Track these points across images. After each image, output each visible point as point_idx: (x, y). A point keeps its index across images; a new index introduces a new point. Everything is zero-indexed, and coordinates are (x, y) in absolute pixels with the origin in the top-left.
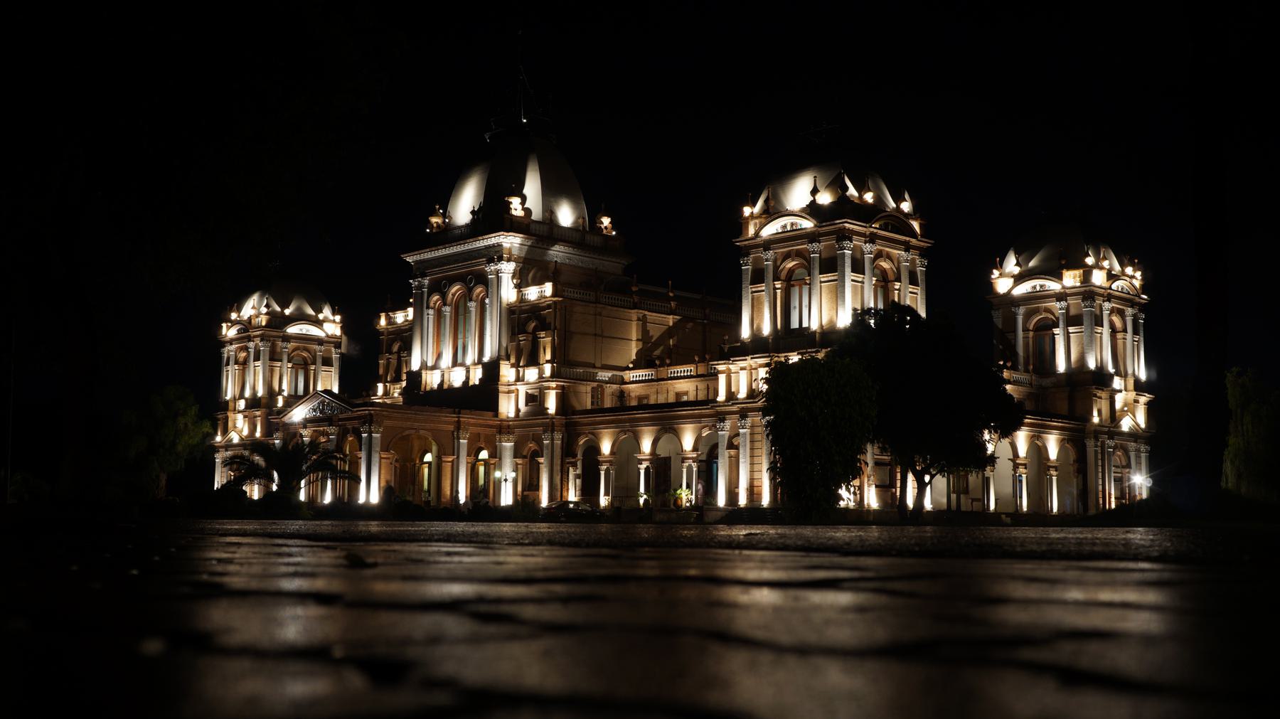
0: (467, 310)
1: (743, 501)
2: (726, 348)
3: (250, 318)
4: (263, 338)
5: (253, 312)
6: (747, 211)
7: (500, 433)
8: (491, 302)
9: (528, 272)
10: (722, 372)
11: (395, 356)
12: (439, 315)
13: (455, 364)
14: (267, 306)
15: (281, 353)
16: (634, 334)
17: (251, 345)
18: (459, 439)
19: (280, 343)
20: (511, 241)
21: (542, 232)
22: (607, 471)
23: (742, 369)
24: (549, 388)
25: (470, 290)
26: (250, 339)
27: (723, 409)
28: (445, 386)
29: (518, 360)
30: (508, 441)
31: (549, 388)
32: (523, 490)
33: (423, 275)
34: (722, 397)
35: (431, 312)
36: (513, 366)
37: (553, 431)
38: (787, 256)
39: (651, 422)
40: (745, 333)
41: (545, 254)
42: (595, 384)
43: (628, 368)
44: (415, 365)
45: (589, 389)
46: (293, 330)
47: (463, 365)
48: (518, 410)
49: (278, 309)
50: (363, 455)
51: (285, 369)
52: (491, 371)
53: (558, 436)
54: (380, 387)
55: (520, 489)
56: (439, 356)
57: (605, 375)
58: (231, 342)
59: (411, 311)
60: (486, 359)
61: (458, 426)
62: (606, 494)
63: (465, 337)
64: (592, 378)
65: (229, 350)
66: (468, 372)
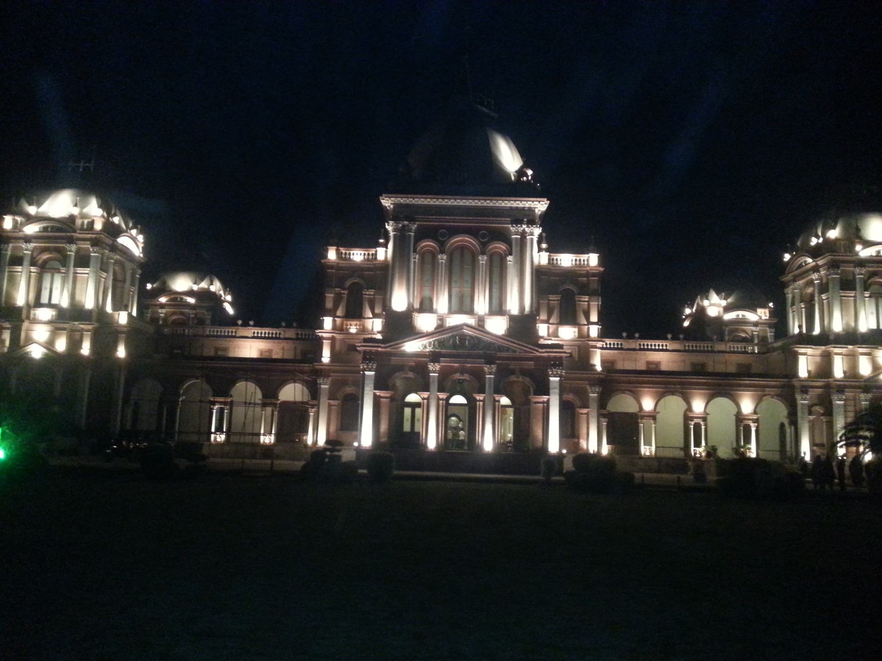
24: (596, 347)
31: (596, 347)
66: (481, 320)
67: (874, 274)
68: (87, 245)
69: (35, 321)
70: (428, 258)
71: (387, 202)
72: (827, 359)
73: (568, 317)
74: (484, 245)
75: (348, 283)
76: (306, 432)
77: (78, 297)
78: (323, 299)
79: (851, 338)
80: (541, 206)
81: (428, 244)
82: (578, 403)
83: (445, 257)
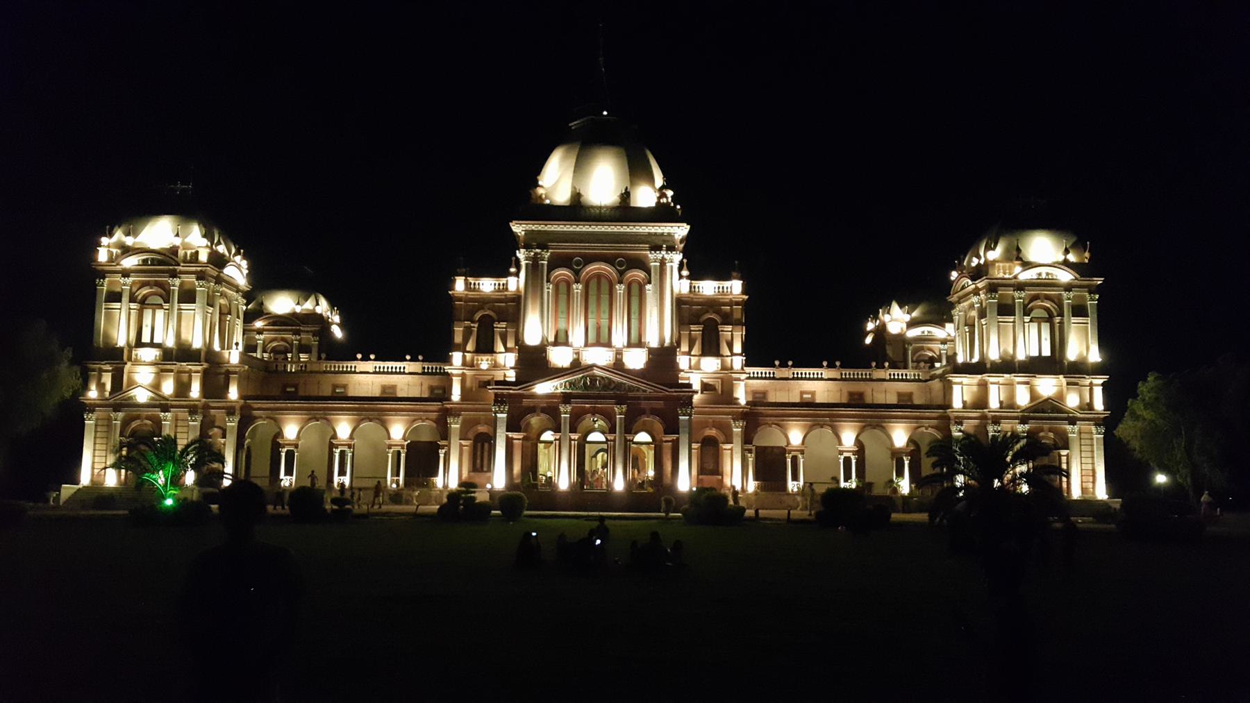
24: (739, 379)
29: (691, 348)
31: (739, 379)
54: (457, 357)
66: (619, 353)
67: (1035, 298)
68: (192, 279)
69: (137, 362)
70: (563, 287)
71: (518, 228)
72: (984, 386)
73: (711, 347)
74: (621, 273)
75: (477, 316)
76: (435, 474)
77: (184, 336)
78: (451, 334)
79: (1007, 366)
80: (680, 231)
82: (721, 438)
83: (580, 286)
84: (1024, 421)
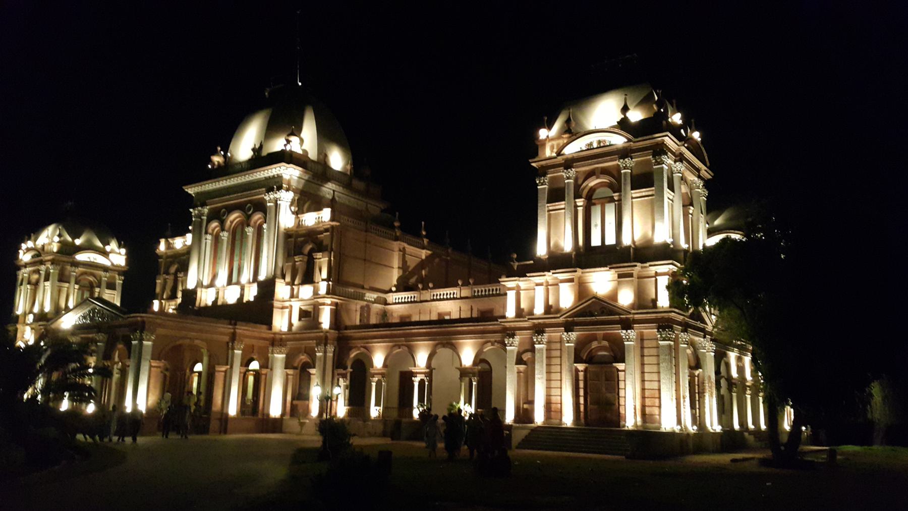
0: (244, 235)
1: (539, 418)
2: (516, 265)
3: (43, 246)
4: (53, 262)
5: (47, 241)
6: (543, 133)
7: (273, 345)
8: (269, 228)
9: (307, 200)
10: (510, 289)
11: (170, 278)
12: (217, 240)
13: (230, 282)
14: (60, 236)
15: (70, 276)
16: (396, 262)
17: (43, 268)
18: (233, 349)
19: (69, 267)
20: (291, 173)
21: (317, 170)
22: (379, 384)
23: (537, 285)
24: (324, 304)
25: (249, 217)
26: (42, 263)
27: (512, 324)
28: (219, 303)
29: (293, 279)
30: (280, 353)
31: (324, 304)
32: (293, 399)
33: (203, 205)
34: (511, 313)
35: (209, 237)
36: (287, 284)
37: (326, 345)
38: (590, 175)
39: (428, 336)
40: (541, 250)
41: (319, 190)
42: (365, 303)
43: (391, 291)
44: (191, 284)
45: (358, 307)
46: (81, 257)
47: (238, 283)
48: (291, 325)
49: (70, 239)
50: (131, 363)
51: (71, 290)
52: (267, 289)
53: (331, 349)
55: (289, 398)
56: (214, 277)
57: (371, 296)
58: (26, 265)
59: (189, 237)
60: (262, 277)
61: (233, 337)
62: (377, 404)
63: (240, 259)
64: (361, 297)
65: (24, 273)
66: (243, 289)
81: (214, 224)
84: (568, 327)
